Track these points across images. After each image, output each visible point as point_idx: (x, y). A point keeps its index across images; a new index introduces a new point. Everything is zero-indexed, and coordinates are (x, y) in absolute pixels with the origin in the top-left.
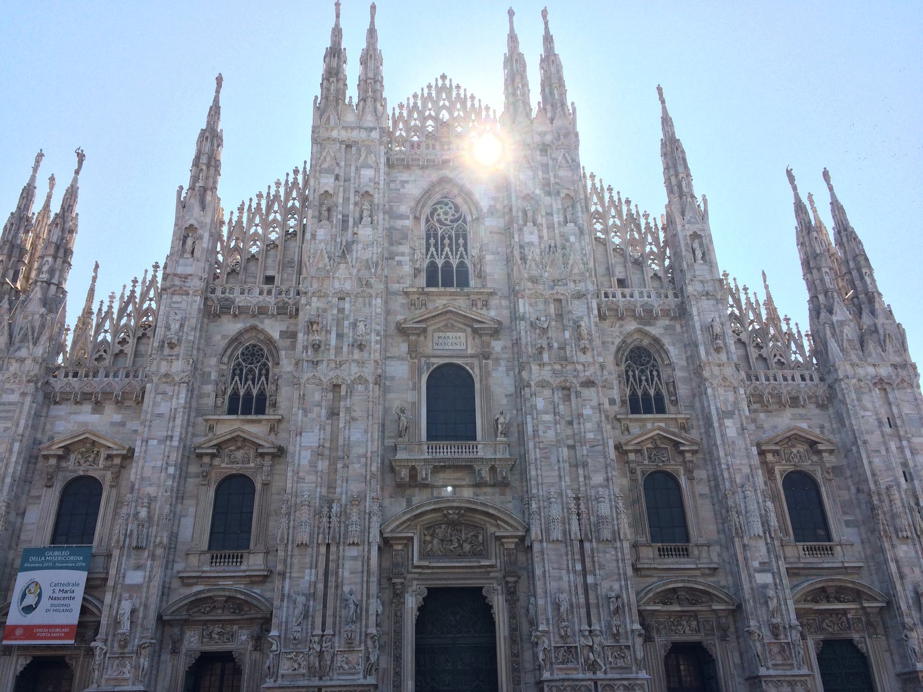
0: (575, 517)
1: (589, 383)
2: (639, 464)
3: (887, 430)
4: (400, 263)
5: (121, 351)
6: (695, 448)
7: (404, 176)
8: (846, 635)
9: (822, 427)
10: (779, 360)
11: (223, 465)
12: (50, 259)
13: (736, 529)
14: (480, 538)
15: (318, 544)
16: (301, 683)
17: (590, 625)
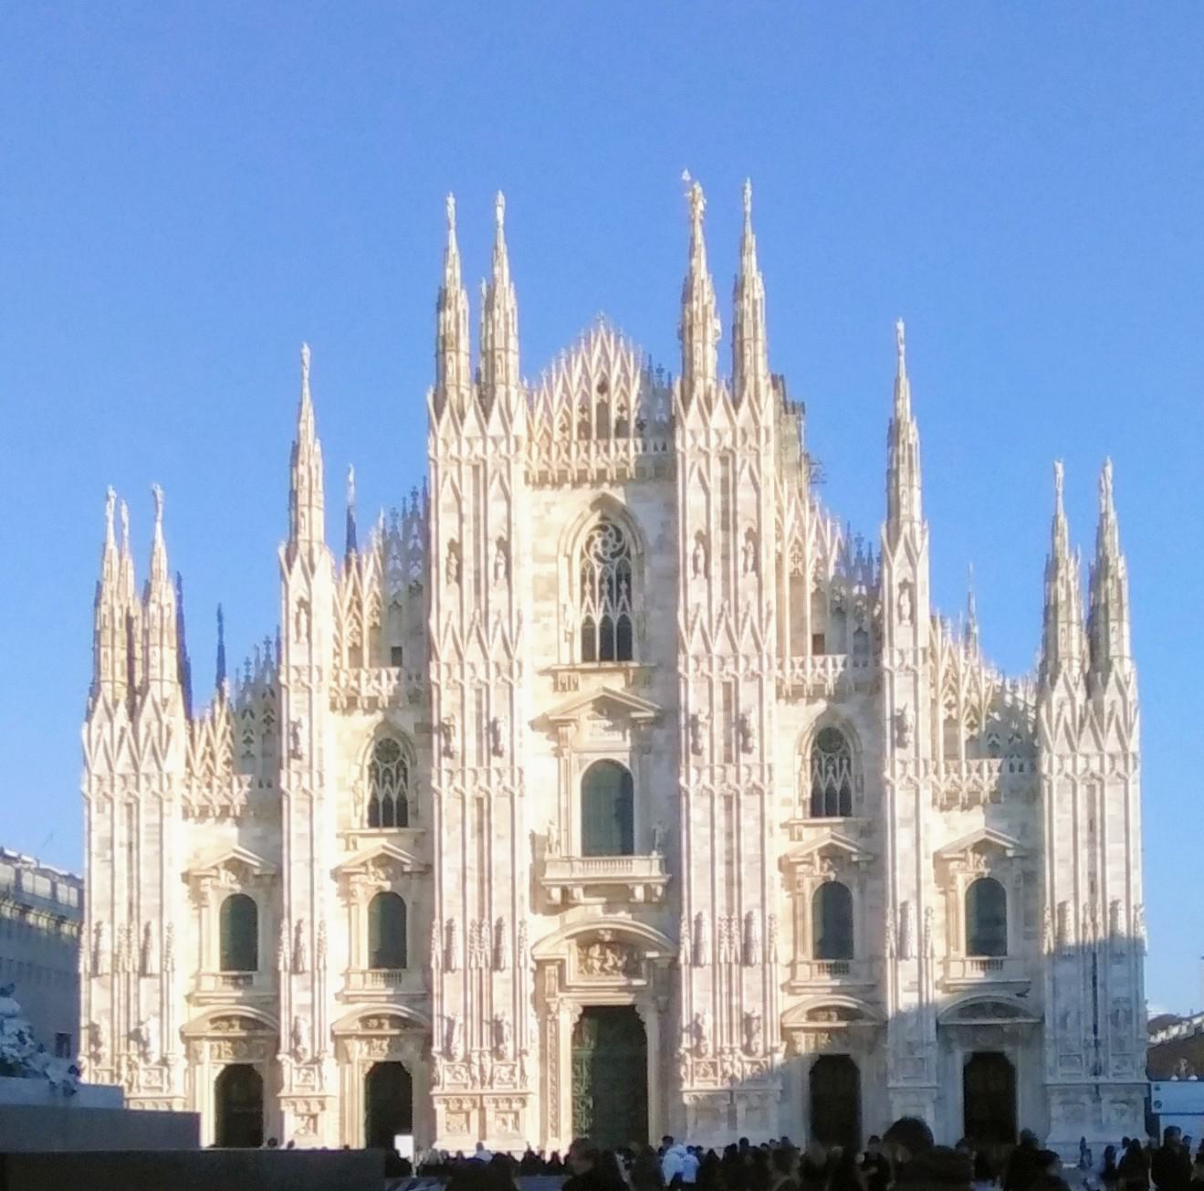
0: (725, 940)
1: (757, 790)
2: (810, 874)
3: (1083, 835)
4: (546, 627)
5: (248, 752)
6: (870, 858)
7: (548, 493)
8: (998, 1049)
9: (1024, 826)
10: (993, 742)
11: (369, 882)
12: (157, 649)
13: (891, 950)
14: (636, 956)
15: (471, 970)
16: (464, 1091)
17: (731, 1042)
